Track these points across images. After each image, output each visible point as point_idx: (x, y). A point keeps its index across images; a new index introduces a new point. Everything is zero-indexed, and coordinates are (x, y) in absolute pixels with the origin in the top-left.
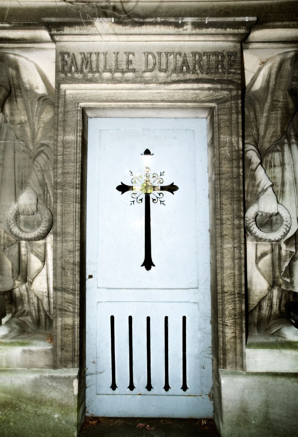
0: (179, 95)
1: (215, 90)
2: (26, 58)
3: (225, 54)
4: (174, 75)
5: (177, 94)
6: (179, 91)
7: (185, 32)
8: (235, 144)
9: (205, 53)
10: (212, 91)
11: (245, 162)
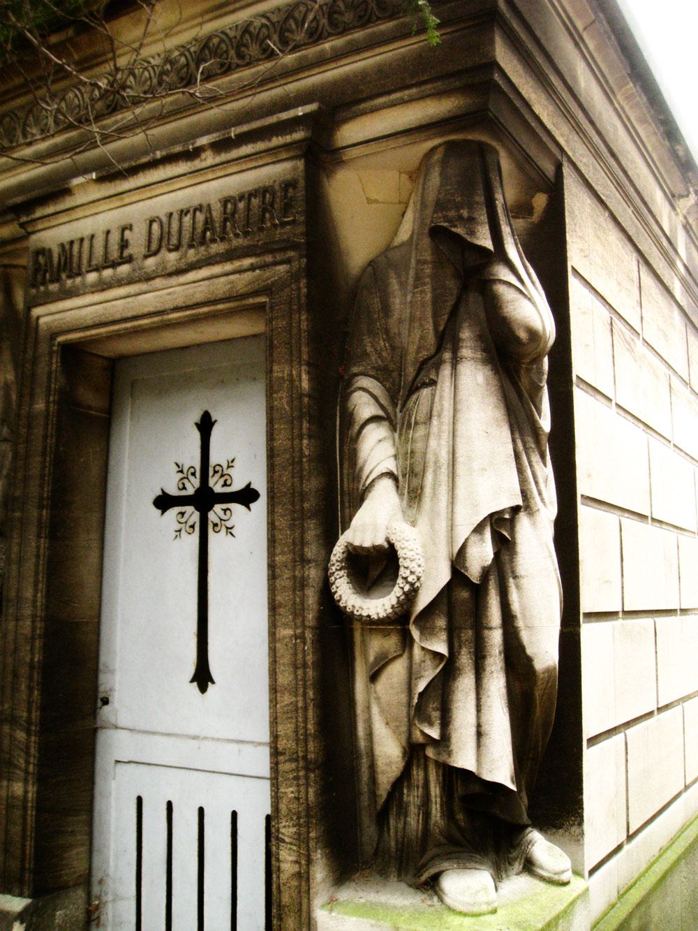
0: (200, 292)
4: (192, 251)
5: (200, 289)
6: (202, 283)
7: (204, 165)
10: (258, 271)
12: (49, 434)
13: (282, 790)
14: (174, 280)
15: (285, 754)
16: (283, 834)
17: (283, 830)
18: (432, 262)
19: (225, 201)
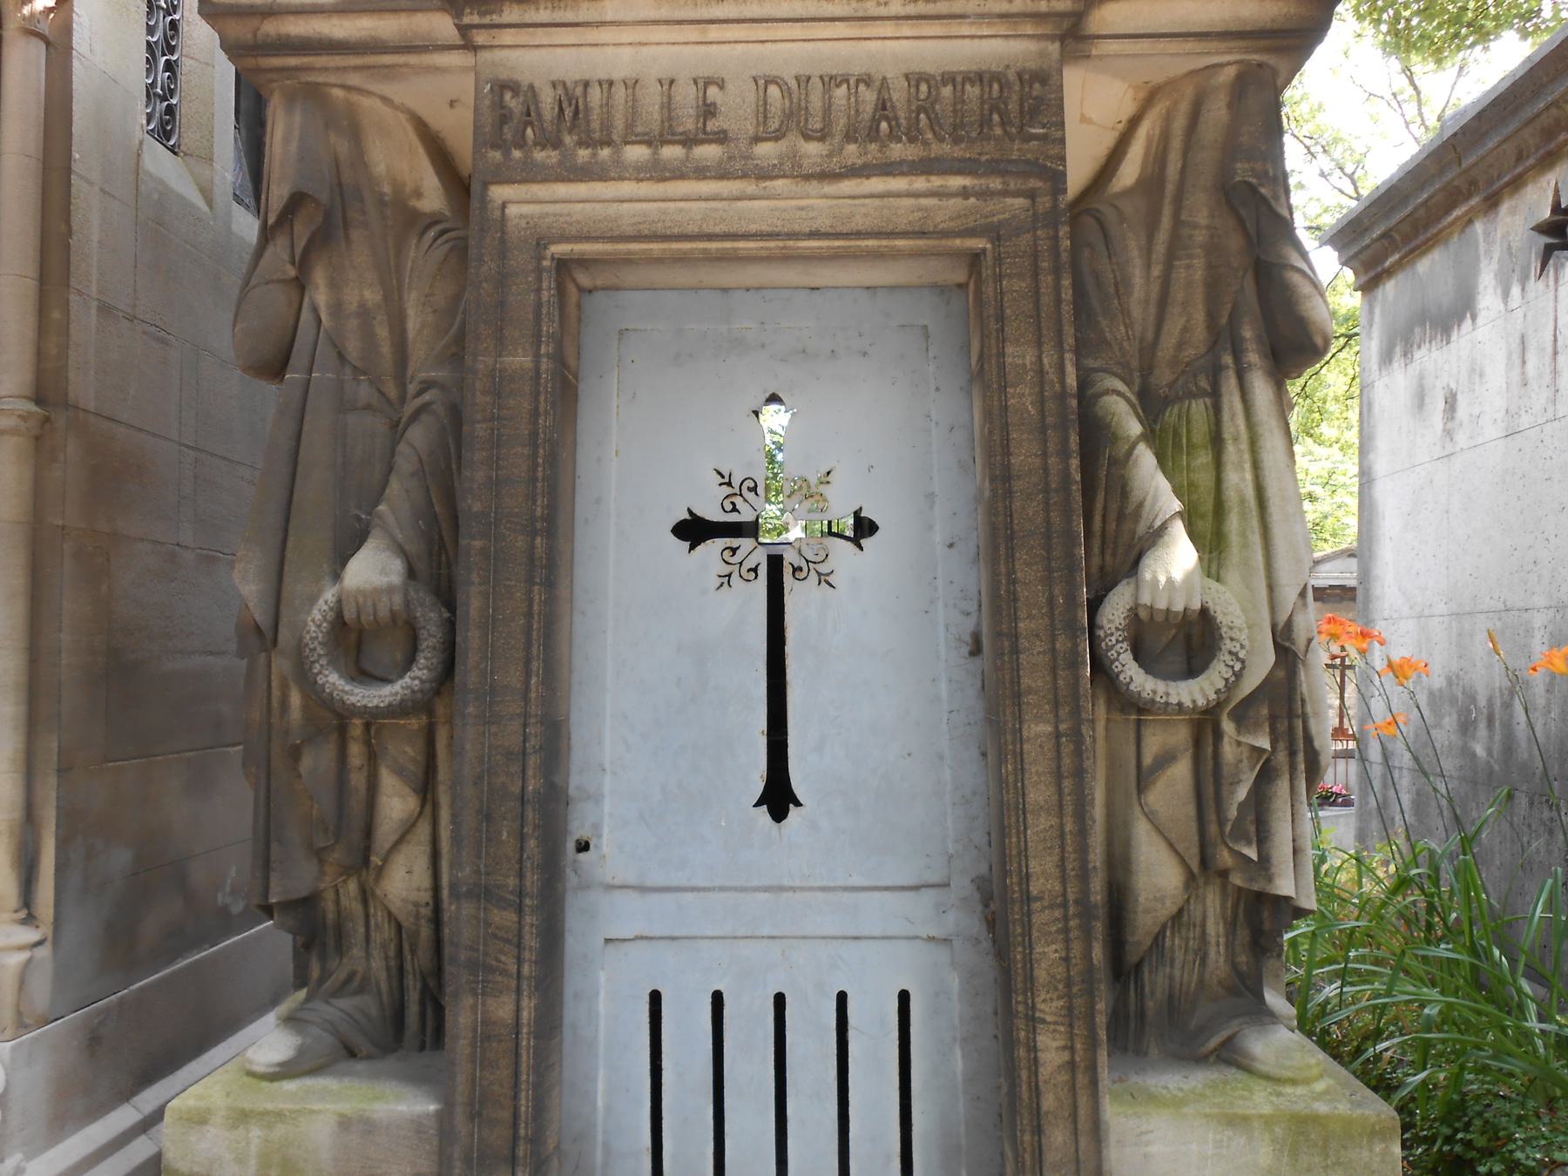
0: (864, 214)
1: (984, 194)
2: (386, 100)
3: (1012, 76)
4: (852, 148)
5: (863, 210)
6: (867, 201)
8: (1052, 375)
9: (949, 78)
10: (972, 200)
11: (1094, 435)
12: (541, 410)
13: (1038, 949)
14: (813, 187)
15: (1042, 898)
16: (1042, 1011)
17: (1040, 1006)
18: (1208, 227)
19: (915, 79)
